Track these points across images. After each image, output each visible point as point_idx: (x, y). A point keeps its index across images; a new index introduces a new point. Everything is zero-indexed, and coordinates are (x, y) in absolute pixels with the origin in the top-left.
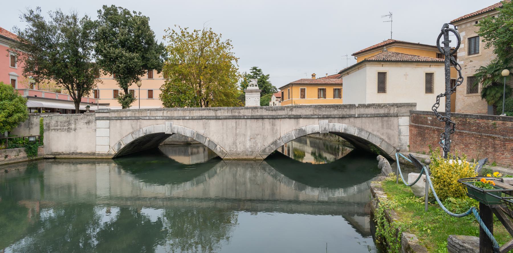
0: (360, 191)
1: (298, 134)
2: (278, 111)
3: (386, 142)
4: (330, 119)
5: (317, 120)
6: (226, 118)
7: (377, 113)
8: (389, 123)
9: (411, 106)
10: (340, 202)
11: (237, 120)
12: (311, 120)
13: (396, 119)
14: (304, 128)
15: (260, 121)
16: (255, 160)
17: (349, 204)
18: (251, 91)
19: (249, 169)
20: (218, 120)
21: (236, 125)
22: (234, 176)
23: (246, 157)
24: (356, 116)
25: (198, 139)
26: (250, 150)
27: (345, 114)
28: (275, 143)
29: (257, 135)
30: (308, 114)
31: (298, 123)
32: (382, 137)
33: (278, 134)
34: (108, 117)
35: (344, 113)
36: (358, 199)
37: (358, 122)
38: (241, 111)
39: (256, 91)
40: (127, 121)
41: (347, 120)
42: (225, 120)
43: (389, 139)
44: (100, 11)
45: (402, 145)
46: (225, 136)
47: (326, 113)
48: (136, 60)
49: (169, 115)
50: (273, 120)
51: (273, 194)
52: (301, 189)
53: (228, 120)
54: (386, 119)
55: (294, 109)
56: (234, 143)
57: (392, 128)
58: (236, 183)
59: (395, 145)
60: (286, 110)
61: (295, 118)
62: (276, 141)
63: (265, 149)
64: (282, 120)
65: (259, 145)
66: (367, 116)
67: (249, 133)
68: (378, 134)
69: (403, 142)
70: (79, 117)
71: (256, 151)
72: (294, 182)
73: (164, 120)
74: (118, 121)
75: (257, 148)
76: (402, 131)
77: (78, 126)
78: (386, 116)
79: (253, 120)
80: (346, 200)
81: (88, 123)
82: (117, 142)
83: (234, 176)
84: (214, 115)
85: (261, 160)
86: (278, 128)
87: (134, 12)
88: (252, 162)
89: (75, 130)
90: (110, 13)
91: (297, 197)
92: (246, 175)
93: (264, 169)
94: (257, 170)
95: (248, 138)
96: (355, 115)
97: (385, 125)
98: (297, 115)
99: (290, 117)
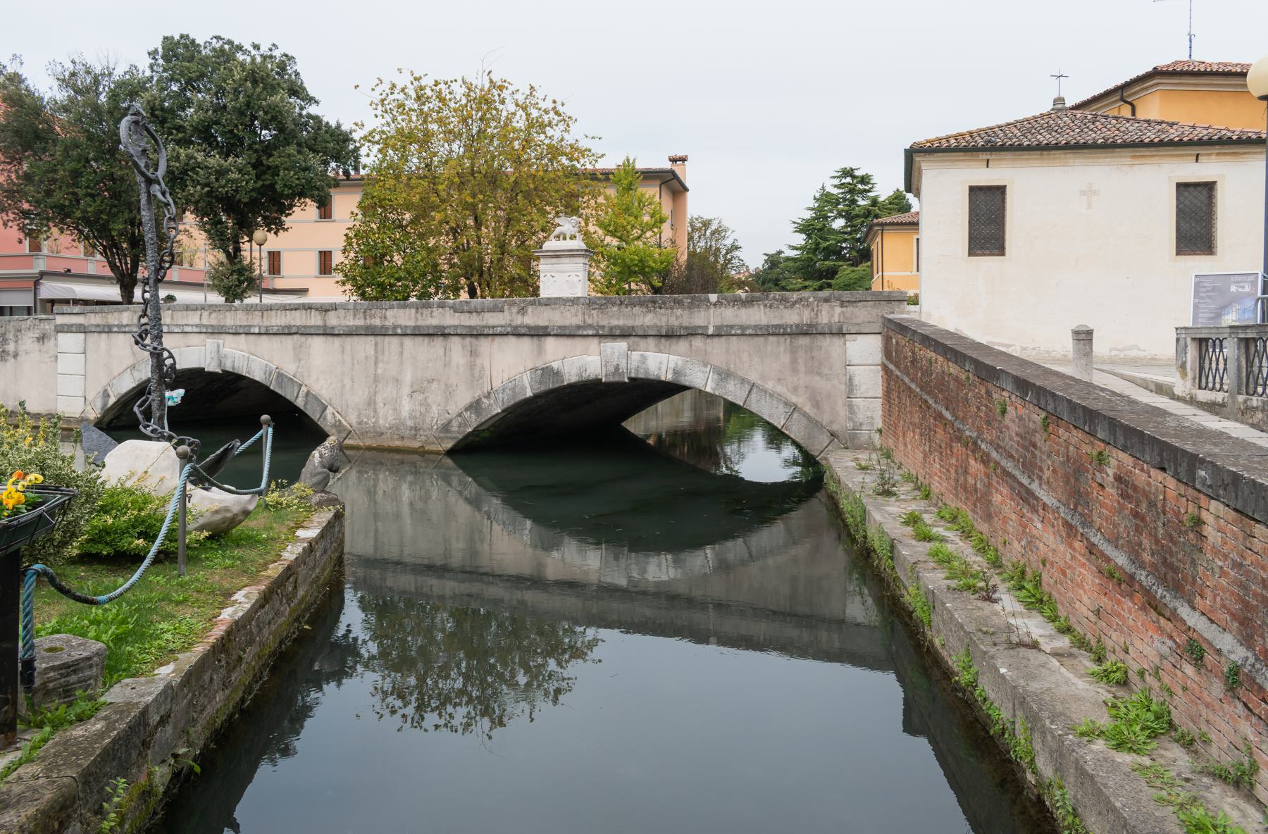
0: (723, 566)
1: (540, 383)
2: (487, 315)
3: (805, 414)
4: (632, 339)
5: (596, 340)
6: (351, 333)
7: (776, 322)
8: (815, 353)
9: (889, 301)
10: (669, 596)
11: (379, 339)
12: (578, 343)
13: (837, 341)
14: (555, 365)
15: (439, 341)
16: (422, 453)
17: (691, 602)
18: (556, 255)
19: (410, 478)
20: (330, 338)
21: (376, 352)
22: (371, 493)
23: (398, 443)
24: (710, 332)
25: (281, 388)
26: (410, 423)
27: (676, 323)
28: (475, 406)
29: (431, 381)
30: (567, 323)
31: (540, 351)
32: (794, 399)
33: (486, 380)
34: (81, 325)
35: (674, 322)
36: (717, 589)
37: (717, 348)
38: (389, 313)
39: (572, 254)
40: (121, 335)
41: (682, 345)
42: (349, 339)
43: (817, 405)
44: (153, 54)
45: (858, 427)
46: (347, 382)
47: (621, 322)
48: (234, 176)
49: (214, 322)
50: (473, 340)
51: (473, 553)
52: (548, 547)
53: (356, 339)
54: (803, 341)
55: (530, 309)
56: (371, 403)
57: (826, 371)
58: (376, 516)
59: (835, 427)
60: (506, 313)
61: (532, 336)
62: (478, 402)
63: (450, 422)
64: (498, 339)
65: (435, 409)
66: (744, 332)
67: (408, 377)
68: (780, 389)
69: (861, 417)
70: (24, 325)
71: (425, 426)
72: (529, 523)
73: (203, 336)
74: (104, 336)
75: (428, 420)
76: (856, 381)
77: (22, 348)
78: (806, 334)
79: (420, 339)
80: (682, 589)
81: (42, 339)
82: (100, 389)
83: (371, 493)
84: (320, 323)
85: (438, 453)
86: (487, 364)
87: (257, 47)
88: (416, 458)
89: (16, 356)
90: (177, 52)
91: (540, 566)
92: (398, 492)
93: (446, 479)
94: (428, 482)
95: (406, 390)
96: (707, 327)
97: (801, 361)
98: (537, 327)
99: (517, 334)
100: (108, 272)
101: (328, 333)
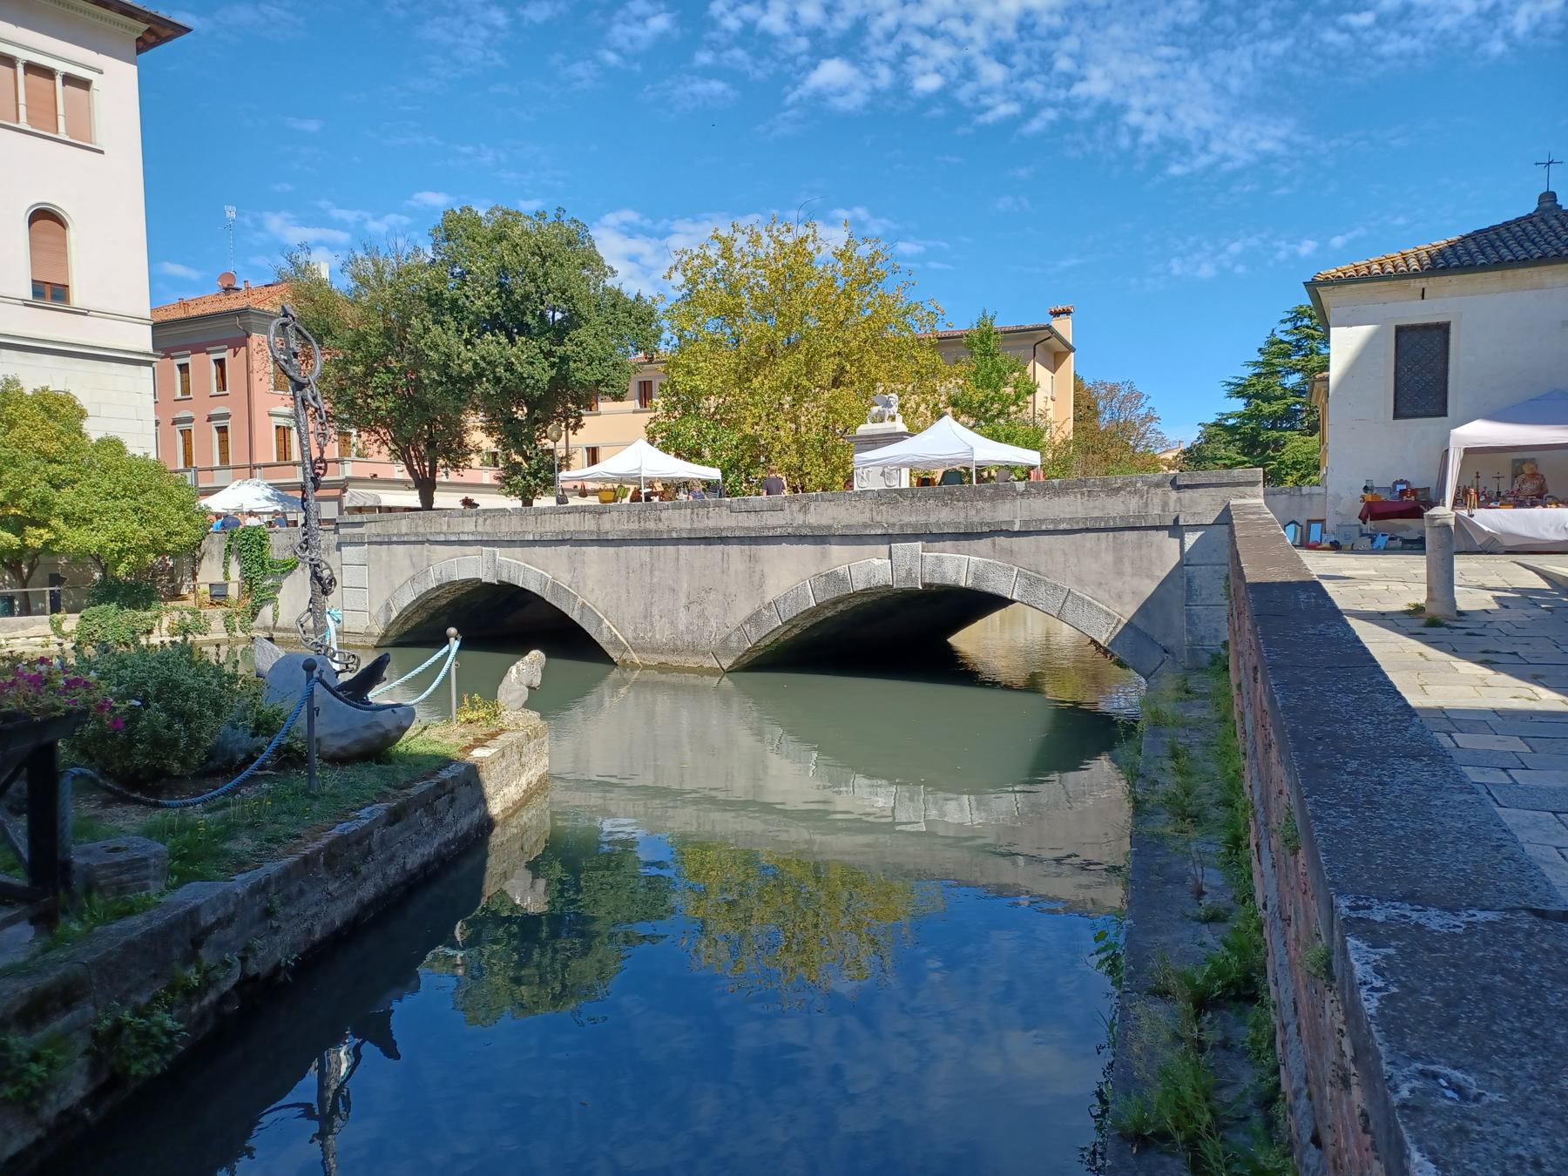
24: (1016, 528)
27: (976, 519)
30: (853, 521)
41: (986, 543)
49: (489, 529)
59: (1169, 642)
60: (787, 511)
62: (758, 613)
65: (713, 623)
75: (706, 634)
76: (1196, 583)
82: (383, 603)
84: (593, 527)
95: (684, 601)
96: (1013, 522)
100: (406, 476)
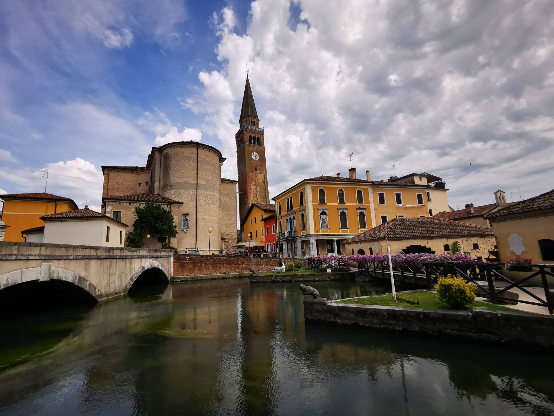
28: (131, 279)
29: (122, 273)
49: (48, 253)
67: (117, 273)
73: (39, 262)
84: (95, 254)
95: (117, 277)
101: (98, 258)
